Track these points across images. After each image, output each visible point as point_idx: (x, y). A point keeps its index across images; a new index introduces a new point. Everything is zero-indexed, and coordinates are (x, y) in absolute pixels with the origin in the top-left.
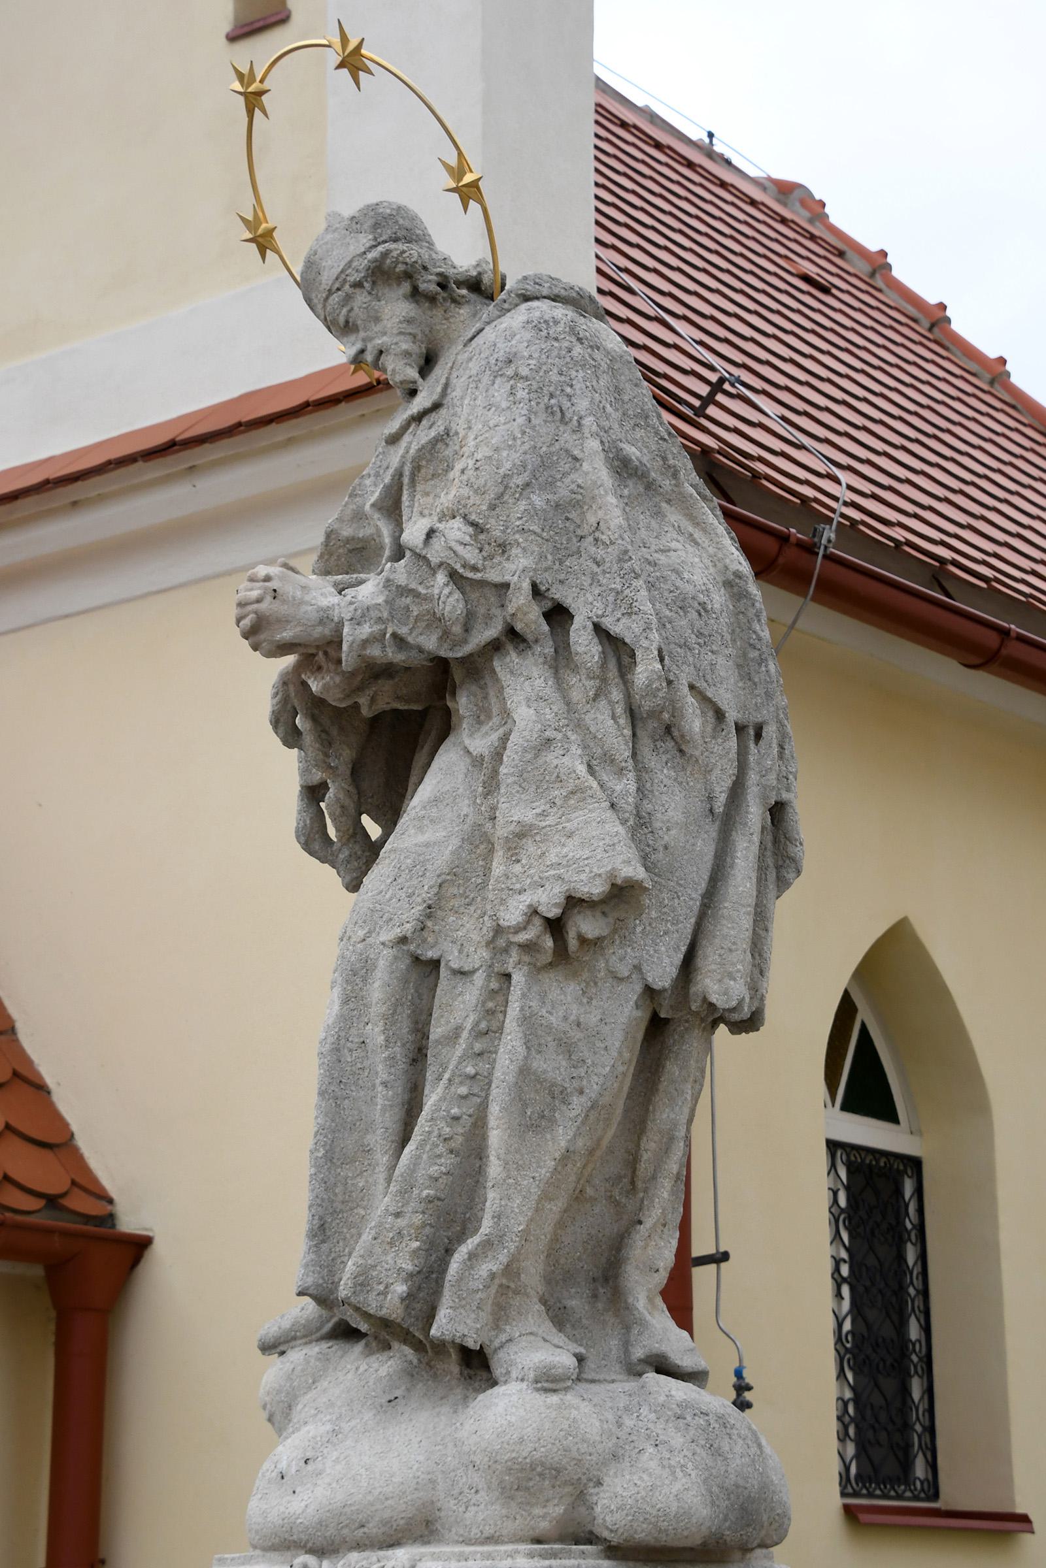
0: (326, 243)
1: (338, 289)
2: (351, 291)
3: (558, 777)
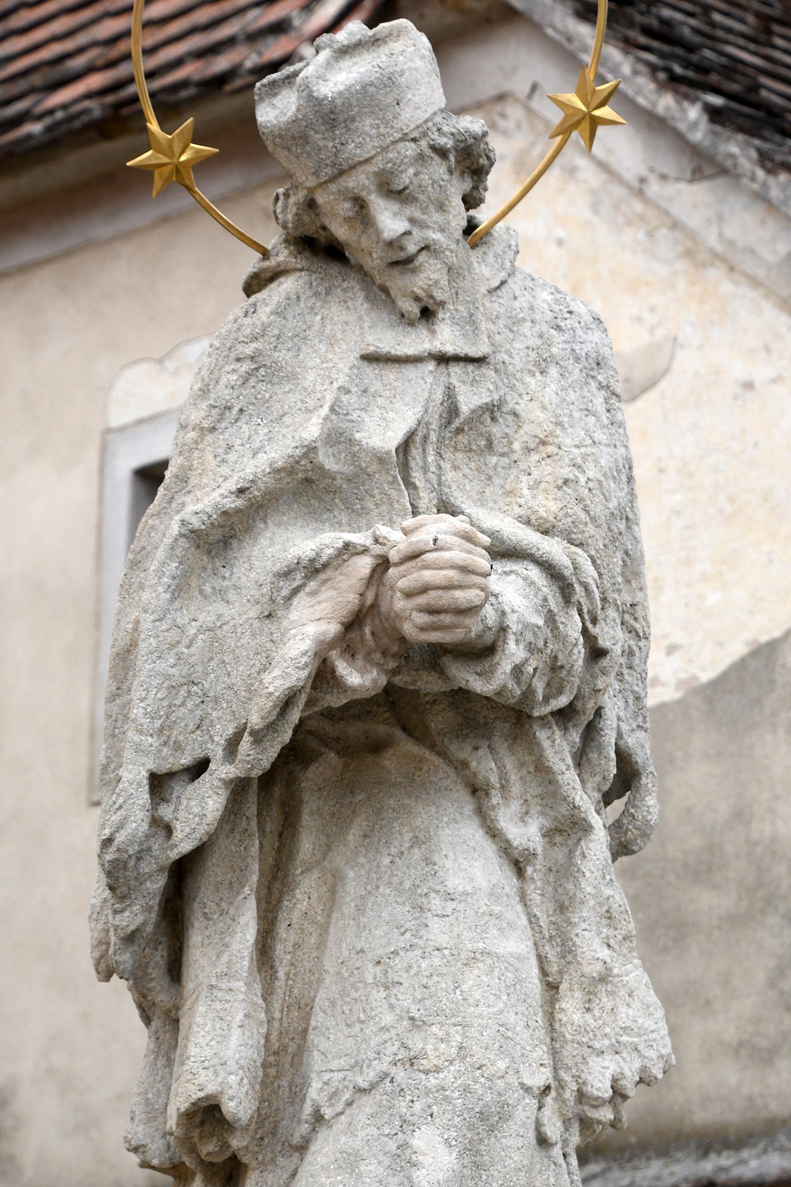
0: (416, 69)
1: (414, 140)
2: (428, 152)
3: (607, 911)
